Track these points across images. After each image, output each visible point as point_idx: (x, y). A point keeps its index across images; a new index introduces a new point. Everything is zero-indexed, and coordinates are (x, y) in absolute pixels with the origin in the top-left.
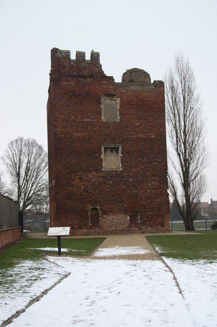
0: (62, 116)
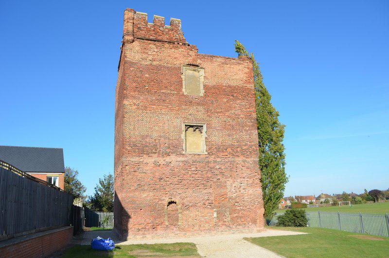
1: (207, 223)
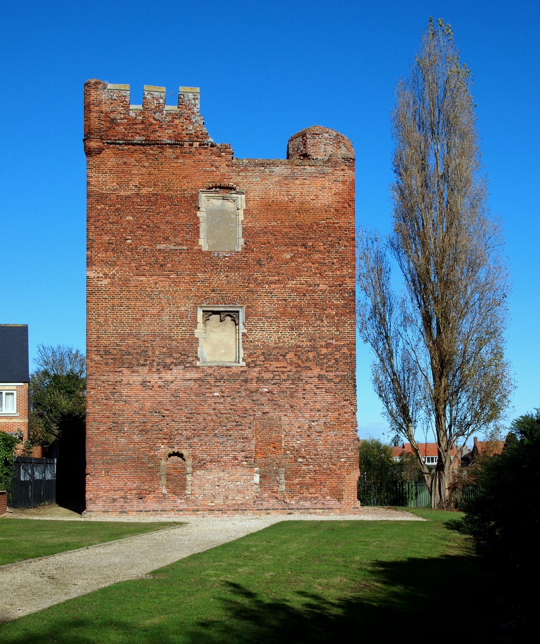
0: (106, 238)
1: (239, 492)
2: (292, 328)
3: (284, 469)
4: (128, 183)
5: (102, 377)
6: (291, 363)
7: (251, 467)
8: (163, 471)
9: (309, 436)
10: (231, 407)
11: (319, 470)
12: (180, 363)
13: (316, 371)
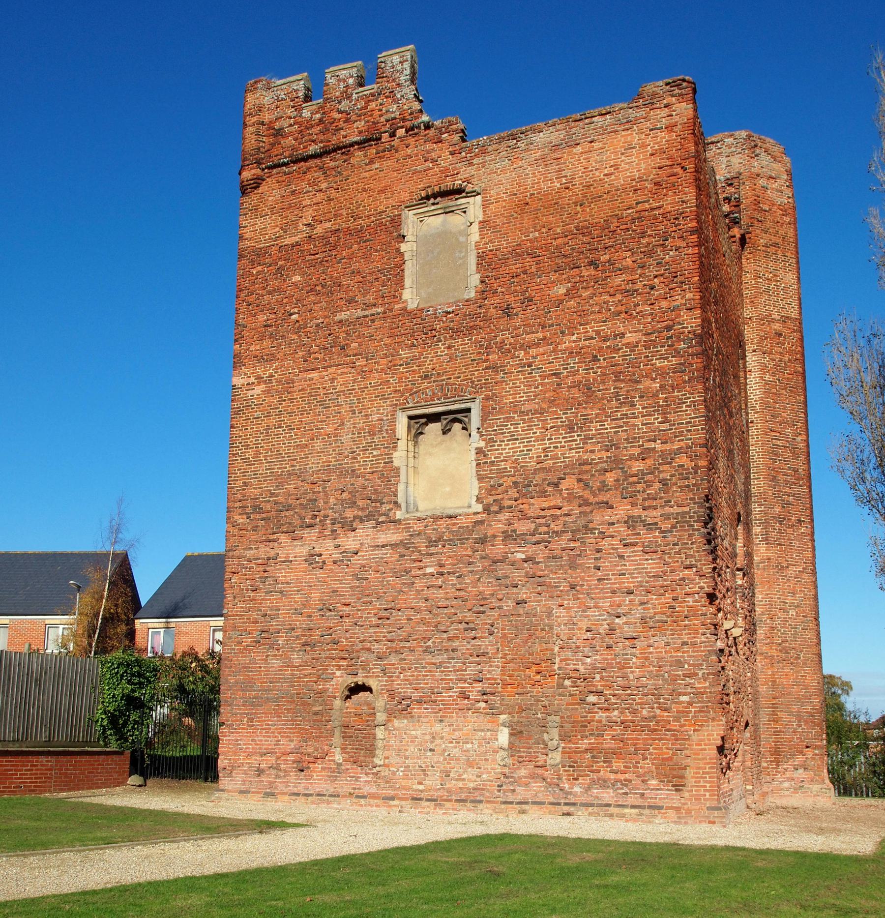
0: (262, 318)
1: (470, 764)
2: (571, 429)
3: (557, 719)
4: (295, 223)
5: (248, 552)
6: (571, 498)
7: (493, 711)
8: (337, 718)
9: (609, 647)
10: (458, 593)
11: (633, 722)
12: (369, 517)
13: (623, 510)
